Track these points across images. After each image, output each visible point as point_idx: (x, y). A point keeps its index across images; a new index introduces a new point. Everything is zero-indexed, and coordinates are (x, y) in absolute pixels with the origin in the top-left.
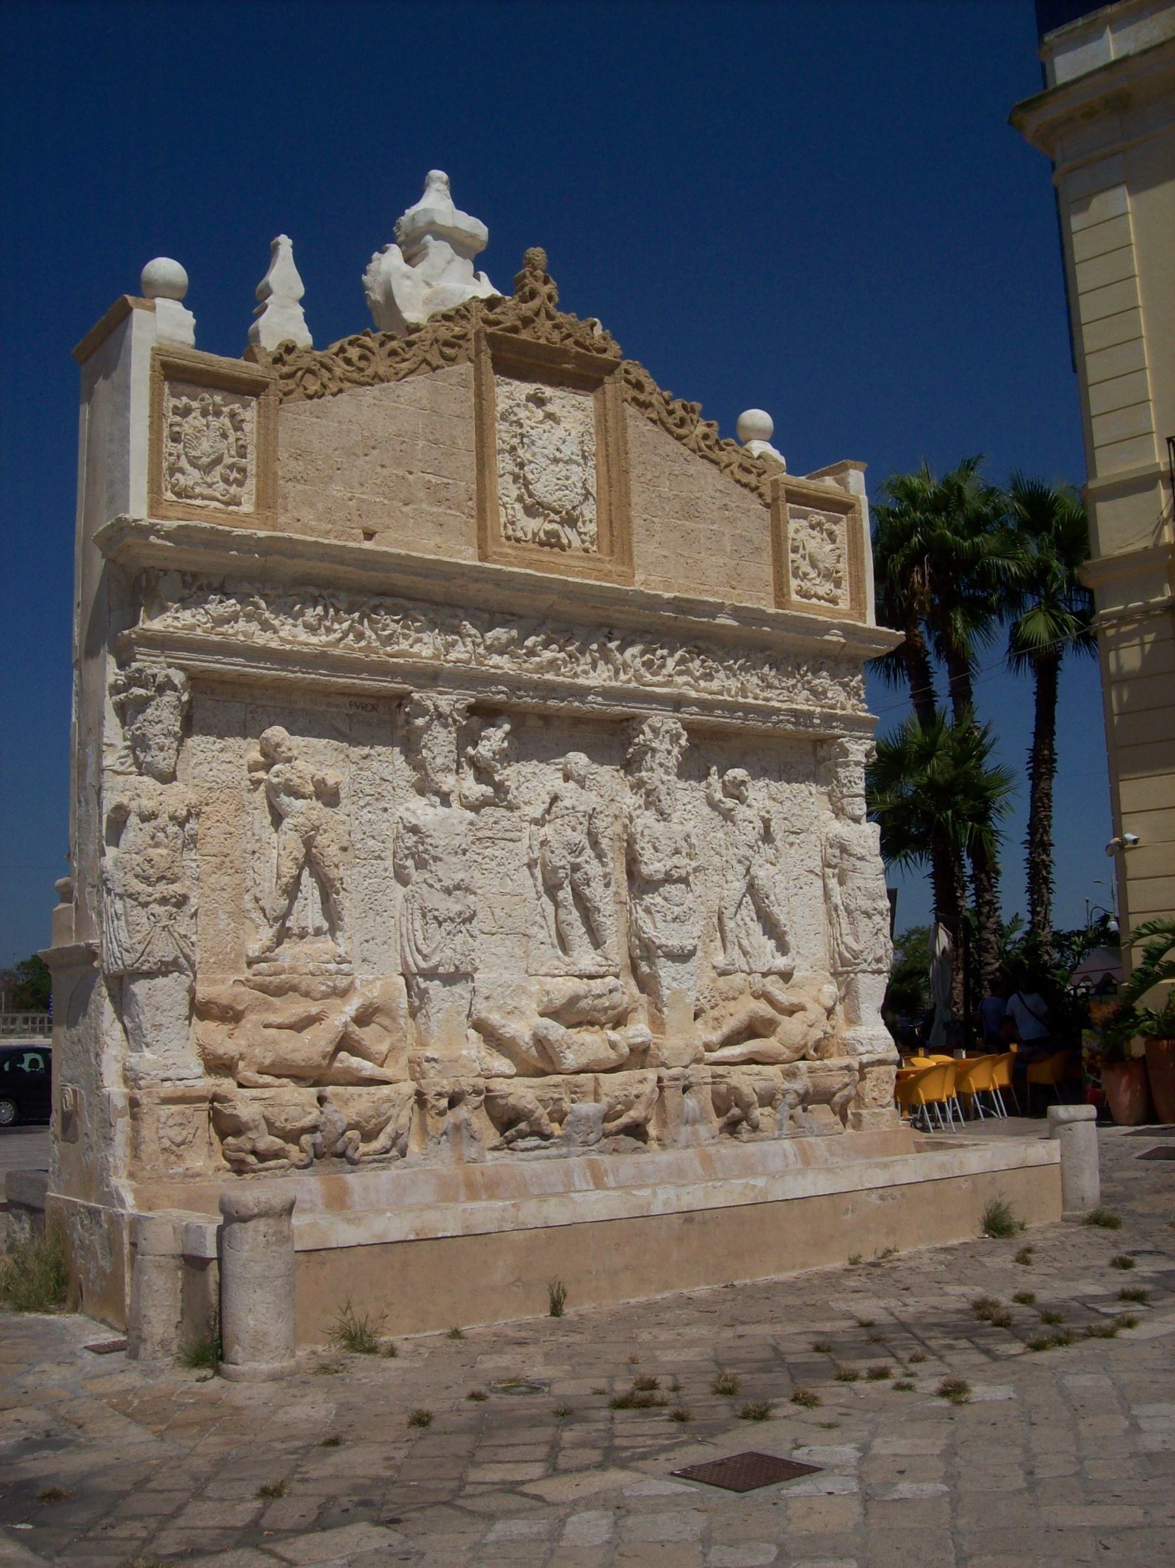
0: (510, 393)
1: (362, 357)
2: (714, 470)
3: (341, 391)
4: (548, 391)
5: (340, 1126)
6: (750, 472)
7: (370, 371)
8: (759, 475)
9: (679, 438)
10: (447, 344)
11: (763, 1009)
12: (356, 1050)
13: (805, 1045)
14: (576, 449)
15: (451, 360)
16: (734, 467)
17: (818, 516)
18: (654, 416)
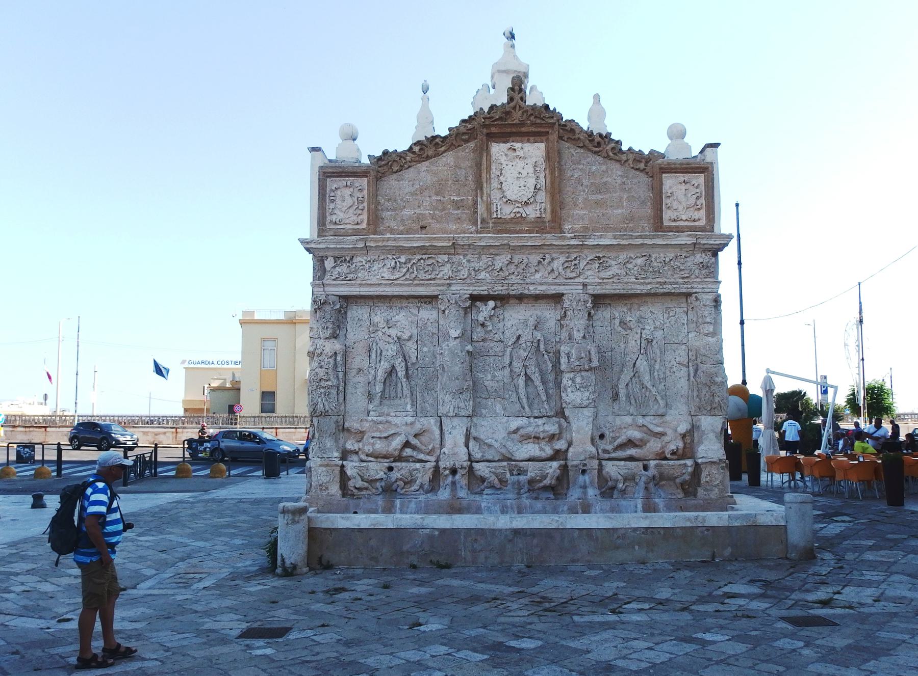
0: (498, 149)
1: (421, 150)
2: (618, 165)
3: (409, 167)
4: (517, 145)
5: (393, 480)
6: (641, 162)
7: (425, 155)
8: (647, 162)
9: (595, 153)
10: (464, 134)
11: (636, 434)
12: (414, 448)
13: (663, 452)
14: (531, 170)
15: (467, 141)
16: (630, 162)
17: (681, 177)
18: (581, 145)
